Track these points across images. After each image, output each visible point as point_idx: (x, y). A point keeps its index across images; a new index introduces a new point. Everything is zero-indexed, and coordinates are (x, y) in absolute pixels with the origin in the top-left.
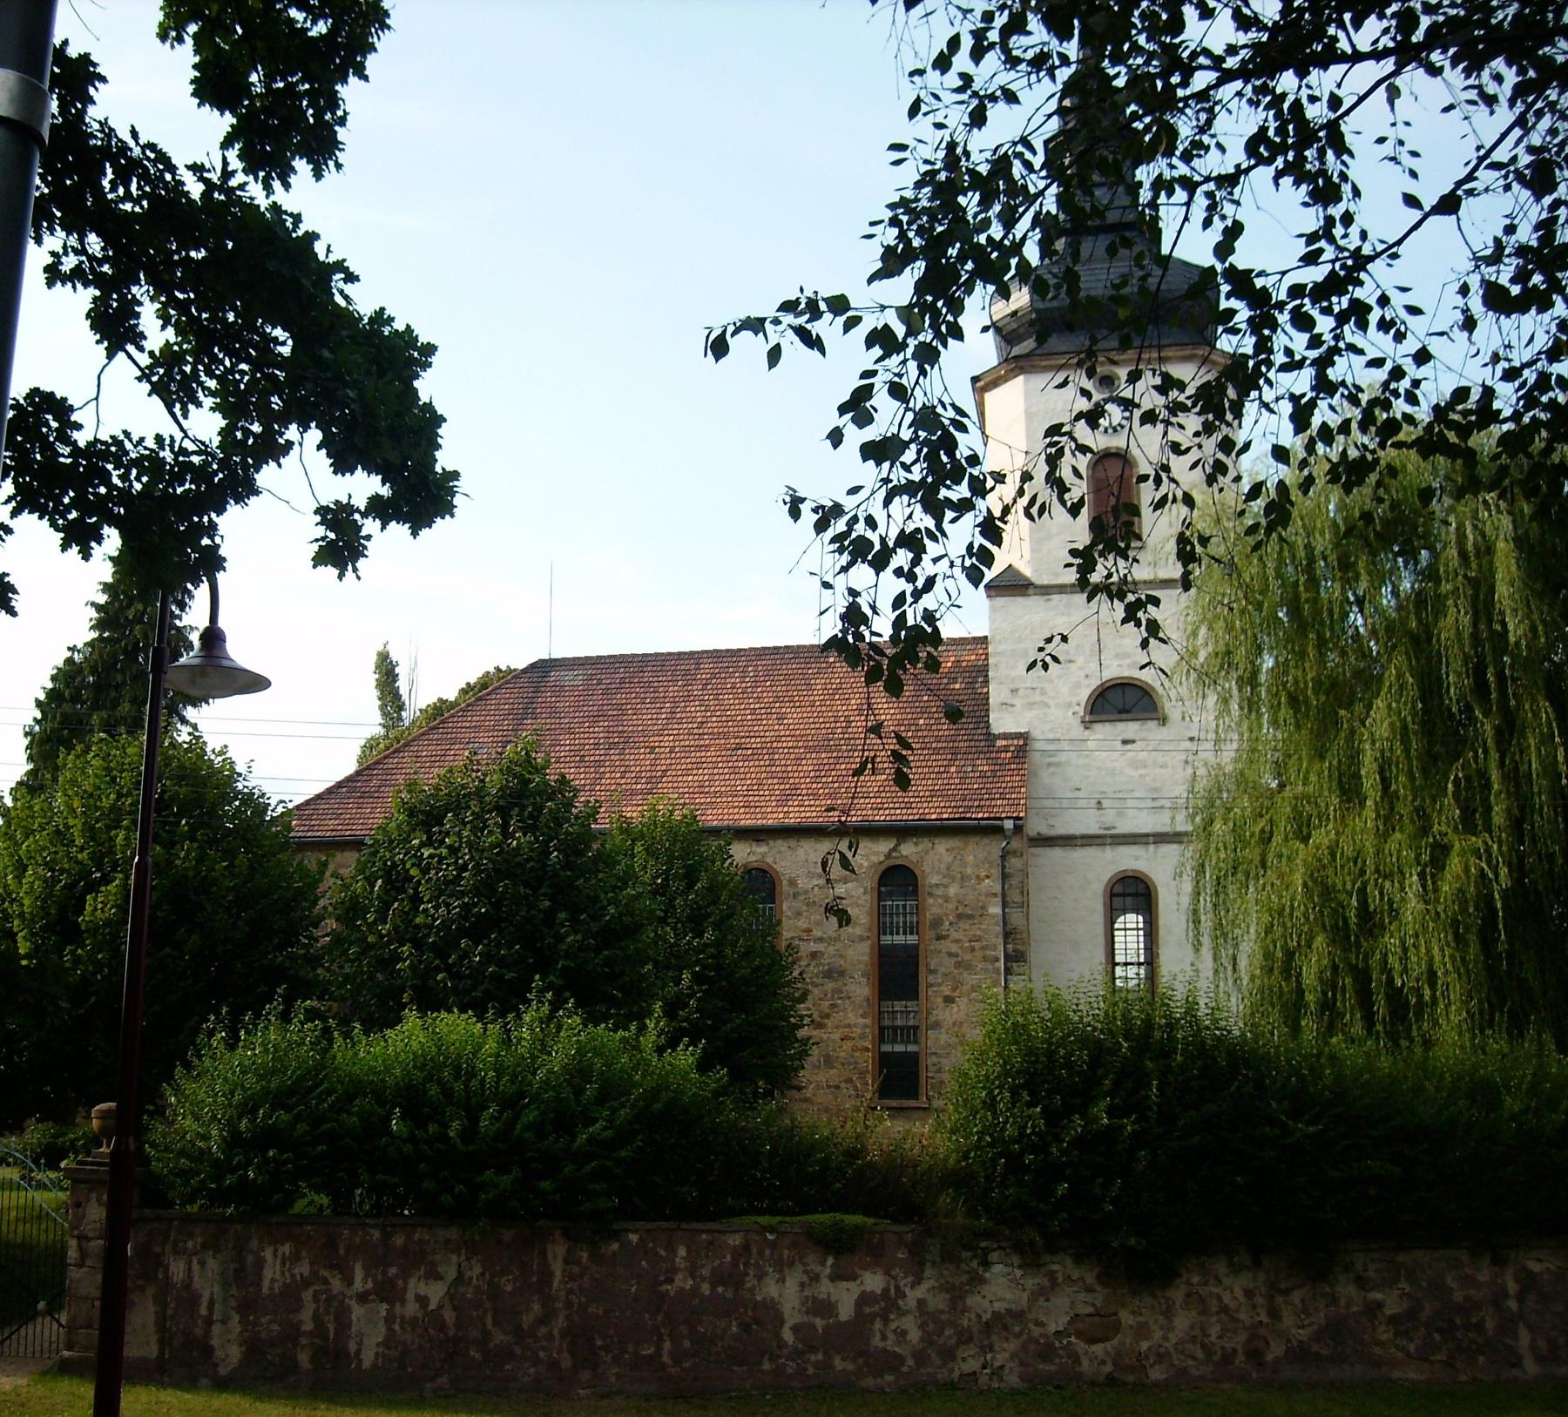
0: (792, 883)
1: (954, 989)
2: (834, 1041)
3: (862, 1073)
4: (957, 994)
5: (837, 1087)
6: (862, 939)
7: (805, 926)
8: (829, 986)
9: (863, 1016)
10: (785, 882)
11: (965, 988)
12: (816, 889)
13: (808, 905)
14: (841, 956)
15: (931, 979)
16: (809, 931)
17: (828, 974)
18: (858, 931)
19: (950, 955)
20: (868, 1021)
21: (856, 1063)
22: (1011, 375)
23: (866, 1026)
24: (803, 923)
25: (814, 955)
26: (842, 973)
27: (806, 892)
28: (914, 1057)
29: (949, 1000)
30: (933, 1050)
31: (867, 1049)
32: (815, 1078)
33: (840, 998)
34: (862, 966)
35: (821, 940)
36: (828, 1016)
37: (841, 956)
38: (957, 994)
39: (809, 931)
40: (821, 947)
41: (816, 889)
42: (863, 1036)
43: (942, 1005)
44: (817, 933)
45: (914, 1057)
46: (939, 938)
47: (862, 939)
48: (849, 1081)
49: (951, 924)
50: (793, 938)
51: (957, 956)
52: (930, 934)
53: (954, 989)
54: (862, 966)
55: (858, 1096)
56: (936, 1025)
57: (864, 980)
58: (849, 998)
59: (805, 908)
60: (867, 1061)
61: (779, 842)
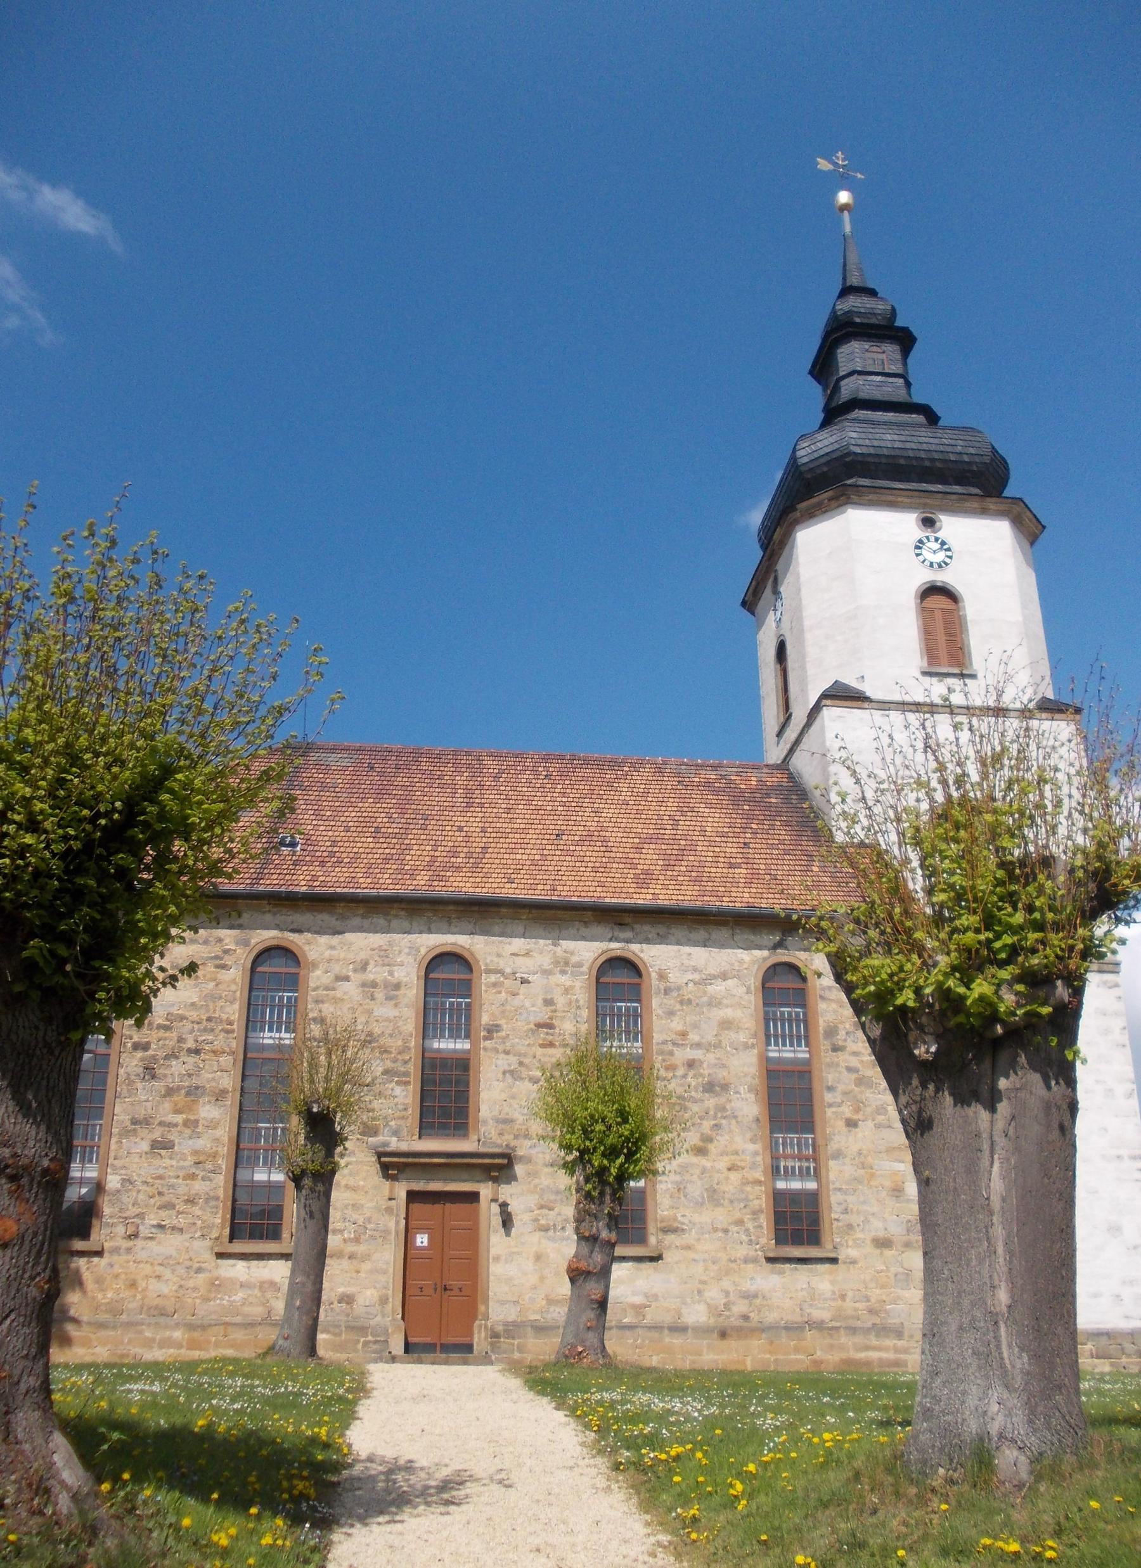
0: (662, 976)
1: (857, 1110)
2: (718, 1171)
3: (755, 1213)
4: (860, 1116)
5: (726, 1231)
6: (746, 1047)
7: (680, 1028)
8: (711, 1102)
9: (753, 1141)
10: (654, 975)
11: (869, 1110)
12: (691, 985)
13: (681, 1002)
14: (724, 1066)
15: (829, 1097)
16: (684, 1034)
17: (710, 1087)
18: (742, 1037)
19: (849, 1069)
20: (758, 1147)
21: (746, 1199)
22: (834, 504)
23: (756, 1153)
24: (676, 1024)
25: (691, 1064)
26: (725, 1087)
27: (679, 988)
28: (813, 1198)
29: (851, 1124)
30: (837, 1185)
31: (760, 1182)
32: (696, 1218)
33: (725, 1118)
34: (749, 1079)
35: (698, 1045)
36: (710, 1140)
37: (724, 1066)
38: (860, 1116)
39: (684, 1034)
40: (697, 1054)
41: (691, 985)
42: (753, 1166)
43: (845, 1129)
44: (694, 1037)
45: (813, 1198)
46: (836, 1049)
47: (746, 1047)
48: (740, 1222)
49: (847, 1033)
50: (665, 1042)
51: (856, 1071)
52: (824, 1045)
53: (857, 1110)
54: (749, 1079)
55: (750, 1242)
56: (838, 1155)
57: (751, 1097)
58: (735, 1117)
59: (678, 1007)
60: (760, 1199)
61: (647, 928)
